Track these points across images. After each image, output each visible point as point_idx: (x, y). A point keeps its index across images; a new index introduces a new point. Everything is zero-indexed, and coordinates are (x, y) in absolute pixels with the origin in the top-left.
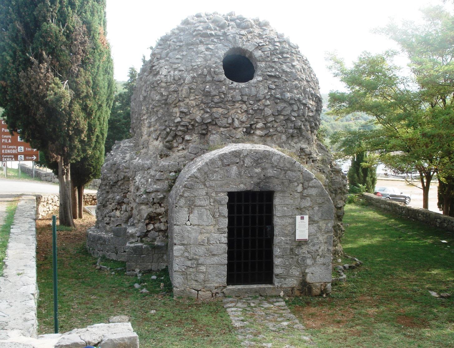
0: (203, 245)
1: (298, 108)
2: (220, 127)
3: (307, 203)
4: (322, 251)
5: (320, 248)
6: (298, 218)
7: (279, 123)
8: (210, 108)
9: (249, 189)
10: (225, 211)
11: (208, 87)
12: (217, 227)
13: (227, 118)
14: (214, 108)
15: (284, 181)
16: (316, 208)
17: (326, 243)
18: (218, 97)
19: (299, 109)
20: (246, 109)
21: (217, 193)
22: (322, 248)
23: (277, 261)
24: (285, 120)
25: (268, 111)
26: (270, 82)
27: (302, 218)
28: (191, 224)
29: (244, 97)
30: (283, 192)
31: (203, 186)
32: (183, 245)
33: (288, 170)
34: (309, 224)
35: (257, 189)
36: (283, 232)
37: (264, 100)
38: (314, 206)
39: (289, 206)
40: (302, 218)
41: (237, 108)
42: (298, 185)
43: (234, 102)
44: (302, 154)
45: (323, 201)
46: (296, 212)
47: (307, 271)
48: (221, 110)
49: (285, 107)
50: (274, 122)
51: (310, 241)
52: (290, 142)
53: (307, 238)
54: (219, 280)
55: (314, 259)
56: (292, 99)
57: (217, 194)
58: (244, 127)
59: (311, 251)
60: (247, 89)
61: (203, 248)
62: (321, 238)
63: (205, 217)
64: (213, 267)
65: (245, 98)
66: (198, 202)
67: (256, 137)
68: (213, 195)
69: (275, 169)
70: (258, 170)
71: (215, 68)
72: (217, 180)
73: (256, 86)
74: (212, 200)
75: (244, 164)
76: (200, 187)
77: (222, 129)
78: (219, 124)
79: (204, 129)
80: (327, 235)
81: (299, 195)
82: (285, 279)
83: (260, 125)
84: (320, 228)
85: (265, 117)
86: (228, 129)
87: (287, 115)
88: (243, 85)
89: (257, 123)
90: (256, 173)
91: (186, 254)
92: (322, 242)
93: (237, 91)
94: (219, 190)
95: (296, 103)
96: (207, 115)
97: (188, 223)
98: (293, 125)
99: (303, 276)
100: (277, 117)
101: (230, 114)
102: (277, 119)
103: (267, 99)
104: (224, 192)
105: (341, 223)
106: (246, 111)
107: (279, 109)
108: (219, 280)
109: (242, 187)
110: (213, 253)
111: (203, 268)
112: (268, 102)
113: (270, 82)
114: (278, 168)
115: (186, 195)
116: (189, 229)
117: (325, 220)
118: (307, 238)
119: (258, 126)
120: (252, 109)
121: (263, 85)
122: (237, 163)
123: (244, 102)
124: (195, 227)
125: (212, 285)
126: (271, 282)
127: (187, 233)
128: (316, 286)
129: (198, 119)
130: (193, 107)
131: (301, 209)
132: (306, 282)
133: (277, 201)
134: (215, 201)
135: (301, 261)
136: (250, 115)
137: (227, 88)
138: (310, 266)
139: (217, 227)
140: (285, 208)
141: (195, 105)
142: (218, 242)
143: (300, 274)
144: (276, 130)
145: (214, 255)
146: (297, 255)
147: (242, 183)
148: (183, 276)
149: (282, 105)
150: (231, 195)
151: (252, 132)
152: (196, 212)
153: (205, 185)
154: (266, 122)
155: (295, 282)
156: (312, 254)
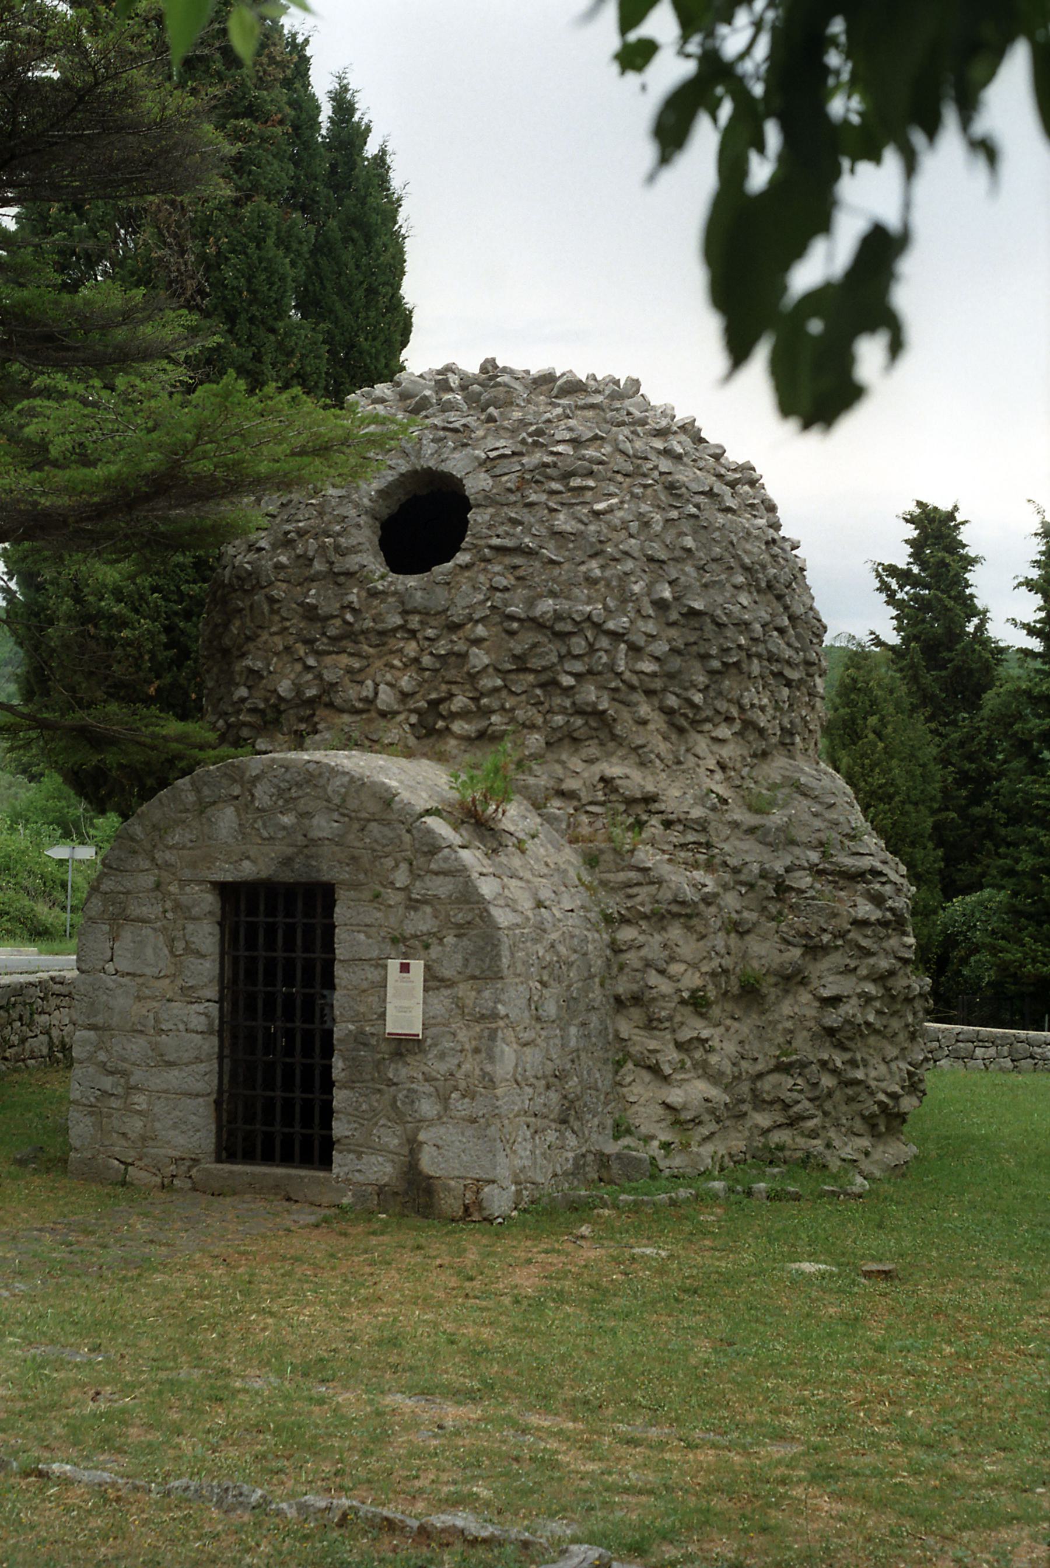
0: (141, 1032)
1: (591, 645)
2: (342, 711)
3: (422, 922)
4: (467, 1076)
5: (459, 1066)
6: (394, 965)
7: (524, 697)
8: (318, 654)
9: (264, 875)
10: (206, 936)
11: (313, 592)
12: (179, 982)
13: (361, 683)
14: (329, 653)
15: (356, 853)
16: (450, 940)
17: (477, 1051)
18: (338, 622)
19: (592, 649)
20: (412, 654)
21: (183, 883)
22: (466, 1067)
23: (340, 1098)
24: (542, 686)
25: (480, 658)
26: (497, 568)
27: (405, 968)
28: (117, 972)
29: (410, 617)
30: (356, 886)
31: (147, 865)
32: (93, 1027)
33: (369, 820)
34: (426, 990)
35: (287, 876)
36: (351, 1008)
37: (469, 626)
38: (444, 932)
39: (372, 931)
40: (405, 968)
41: (391, 652)
42: (397, 866)
43: (382, 633)
44: (613, 797)
45: (469, 918)
46: (388, 948)
47: (421, 1137)
48: (344, 660)
49: (535, 646)
50: (504, 693)
51: (429, 1041)
52: (564, 757)
53: (418, 1029)
54: (181, 1140)
55: (444, 1100)
56: (558, 617)
57: (181, 888)
58: (411, 711)
59: (434, 1074)
60: (419, 594)
61: (142, 1041)
62: (463, 1035)
63: (149, 952)
64: (167, 1099)
65: (414, 622)
66: (134, 910)
67: (453, 742)
68: (173, 889)
69: (336, 816)
70: (287, 820)
71: (339, 534)
72: (184, 848)
73: (448, 584)
74: (169, 905)
75: (252, 801)
76: (142, 867)
77: (346, 718)
78: (338, 701)
79: (301, 720)
80: (482, 1026)
81: (400, 897)
82: (359, 1155)
83: (459, 702)
84: (460, 1005)
85: (473, 677)
86: (364, 716)
87: (545, 669)
88: (412, 581)
89: (451, 696)
90: (284, 828)
91: (102, 1056)
92: (467, 1047)
93: (391, 600)
94: (187, 874)
95: (581, 630)
96: (310, 676)
97: (110, 967)
98: (568, 703)
99: (412, 1151)
100: (513, 676)
101: (371, 671)
102: (515, 682)
103: (477, 621)
104: (200, 882)
105: (847, 1056)
106: (416, 660)
107: (518, 651)
108: (181, 1140)
109: (248, 870)
110: (166, 1058)
111: (140, 1100)
112: (480, 630)
113: (497, 568)
114: (343, 815)
115: (103, 888)
116: (111, 985)
117: (473, 977)
118: (418, 1029)
119: (454, 708)
120: (431, 654)
121: (469, 579)
122: (237, 798)
123: (413, 634)
124: (126, 980)
125: (162, 1151)
126: (326, 1163)
127: (105, 997)
128: (449, 1189)
129: (284, 687)
130: (277, 654)
131: (404, 939)
132: (420, 1173)
133: (344, 912)
134: (177, 907)
135: (404, 1103)
136: (427, 673)
137: (364, 594)
138: (431, 1123)
139: (179, 982)
140: (362, 936)
141: (281, 648)
142: (182, 1027)
143: (401, 1145)
144: (512, 720)
145: (170, 1064)
146: (391, 1083)
147: (248, 858)
148: (93, 1119)
149: (529, 638)
150: (229, 892)
151: (440, 724)
152: (127, 934)
153: (153, 859)
154: (477, 695)
155: (389, 1169)
156: (436, 1084)
